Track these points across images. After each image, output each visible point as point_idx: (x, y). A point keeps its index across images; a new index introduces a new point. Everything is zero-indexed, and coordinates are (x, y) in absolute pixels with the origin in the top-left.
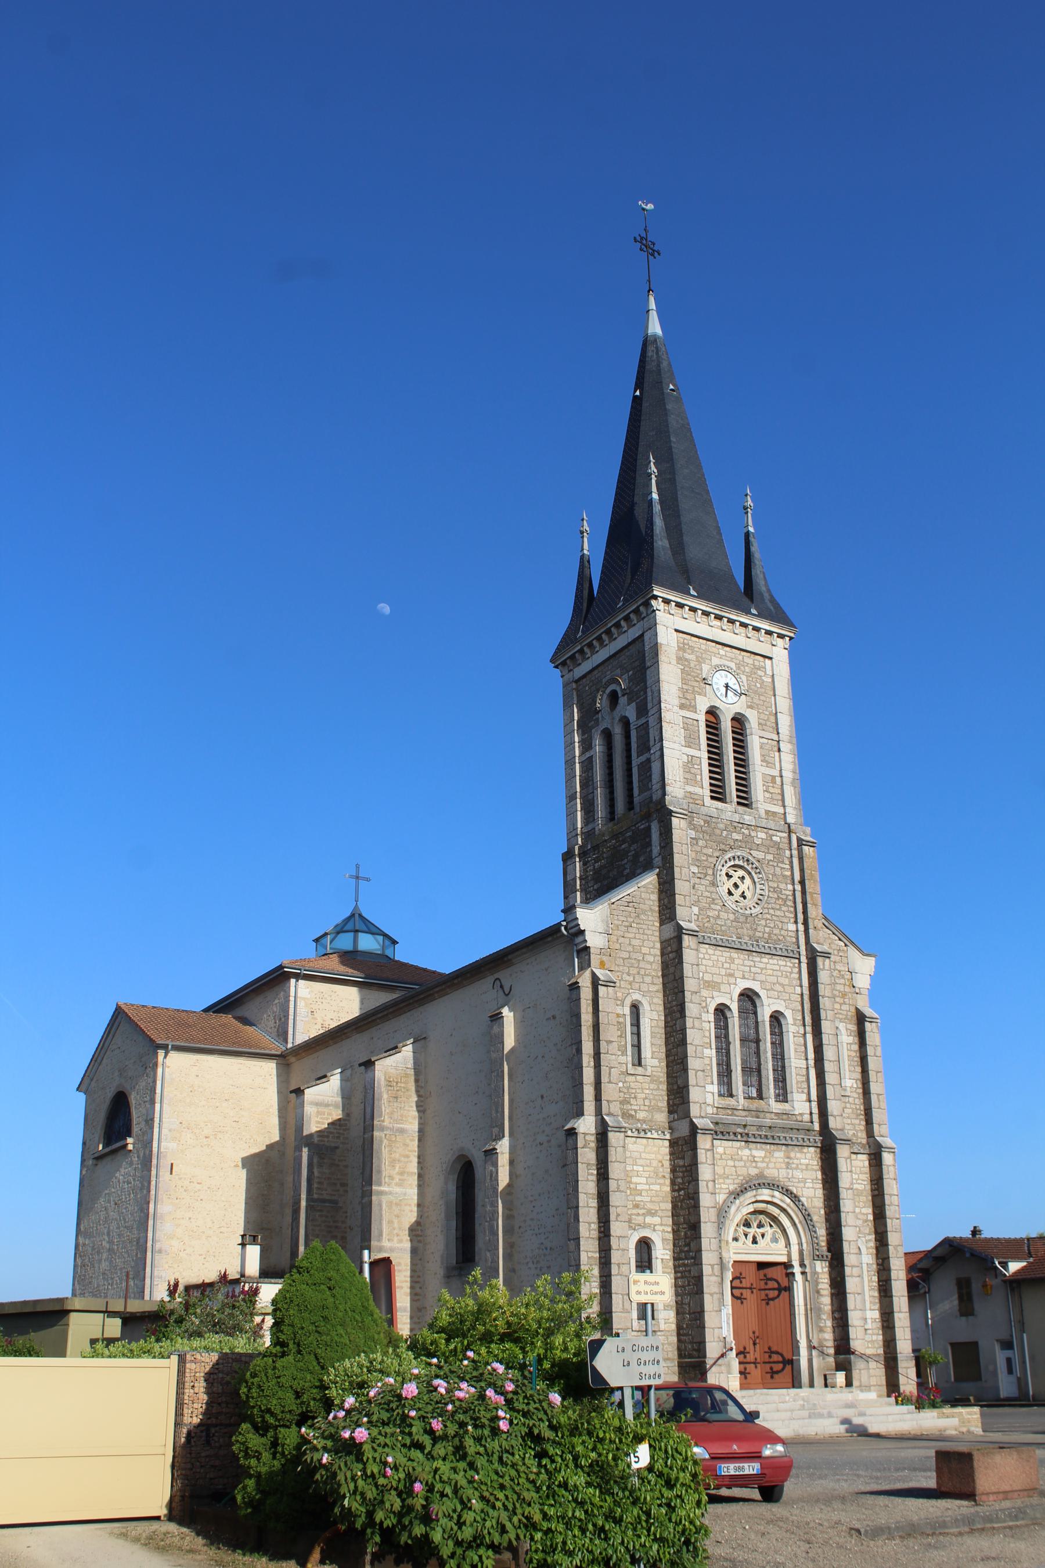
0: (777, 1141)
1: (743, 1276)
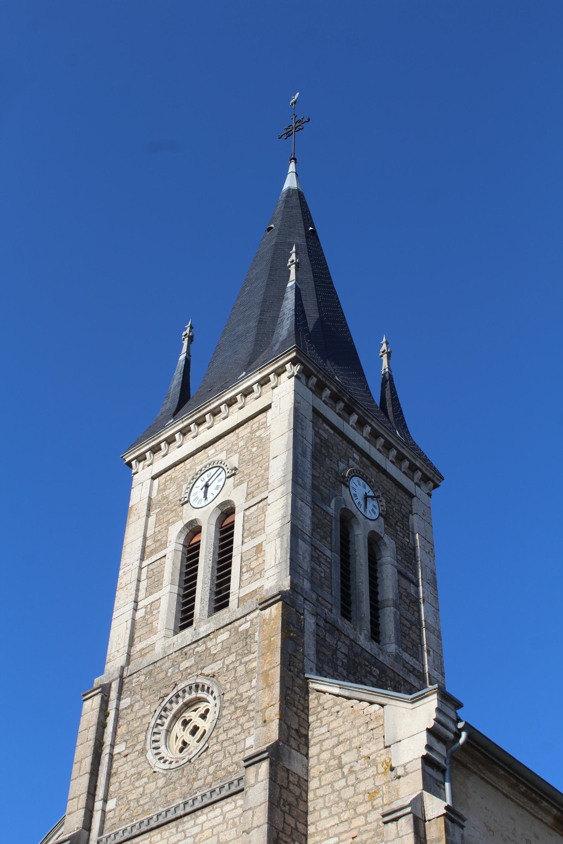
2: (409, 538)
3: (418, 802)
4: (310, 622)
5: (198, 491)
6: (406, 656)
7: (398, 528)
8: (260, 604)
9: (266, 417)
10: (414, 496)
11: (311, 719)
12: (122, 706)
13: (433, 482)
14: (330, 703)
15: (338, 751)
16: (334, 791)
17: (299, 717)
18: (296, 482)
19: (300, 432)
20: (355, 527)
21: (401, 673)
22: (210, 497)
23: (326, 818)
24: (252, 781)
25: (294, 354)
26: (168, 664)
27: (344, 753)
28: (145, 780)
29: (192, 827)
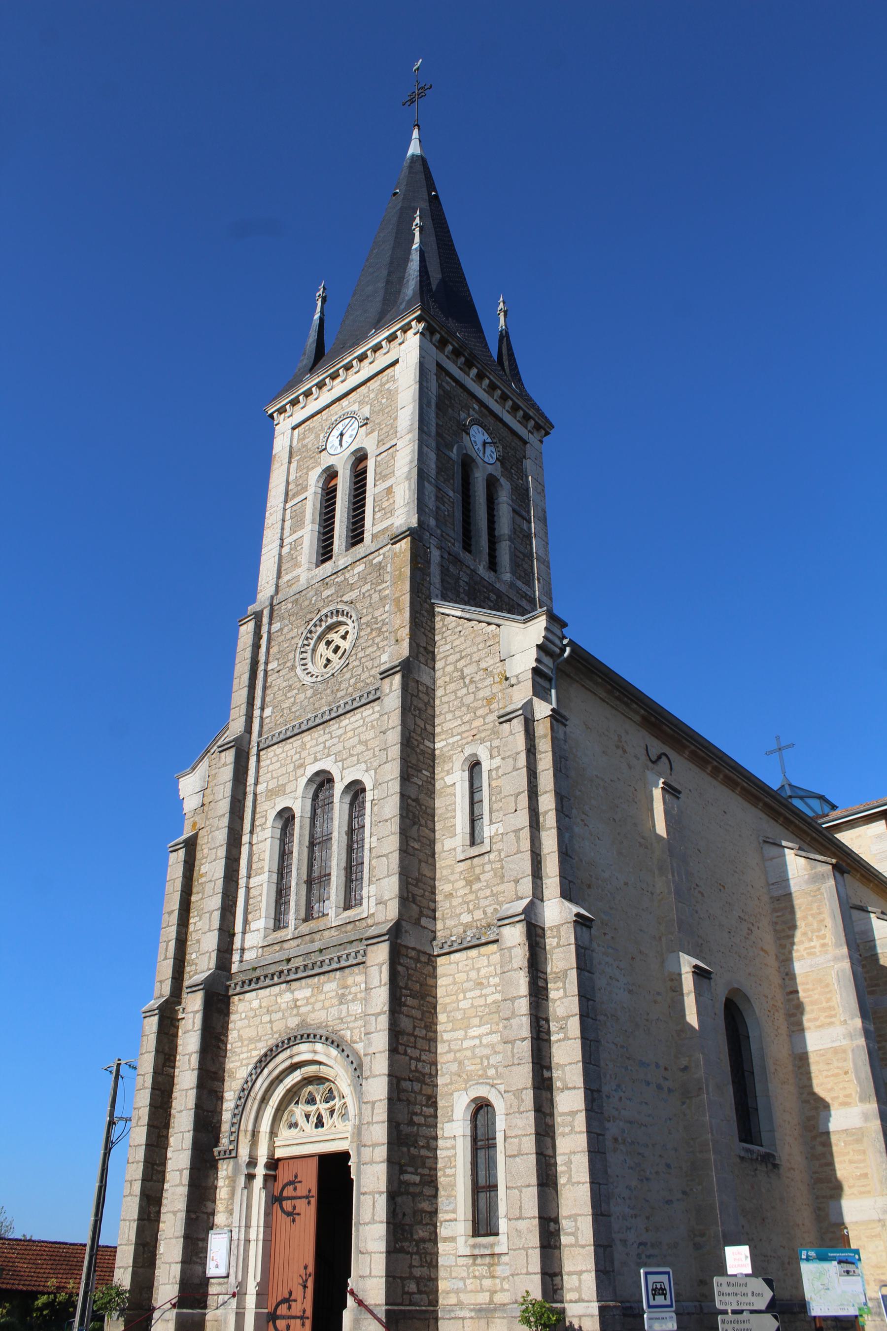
0: (326, 968)
1: (299, 1179)
2: (522, 480)
3: (528, 707)
4: (435, 555)
5: (334, 439)
6: (519, 584)
7: (513, 471)
8: (391, 540)
9: (394, 371)
10: (527, 443)
11: (437, 638)
12: (273, 630)
13: (544, 429)
14: (454, 624)
15: (460, 665)
16: (457, 698)
17: (427, 636)
18: (421, 430)
19: (425, 384)
20: (475, 470)
21: (515, 598)
22: (345, 445)
23: (450, 720)
24: (387, 691)
25: (419, 312)
26: (312, 593)
27: (465, 666)
28: (296, 691)
29: (337, 729)
